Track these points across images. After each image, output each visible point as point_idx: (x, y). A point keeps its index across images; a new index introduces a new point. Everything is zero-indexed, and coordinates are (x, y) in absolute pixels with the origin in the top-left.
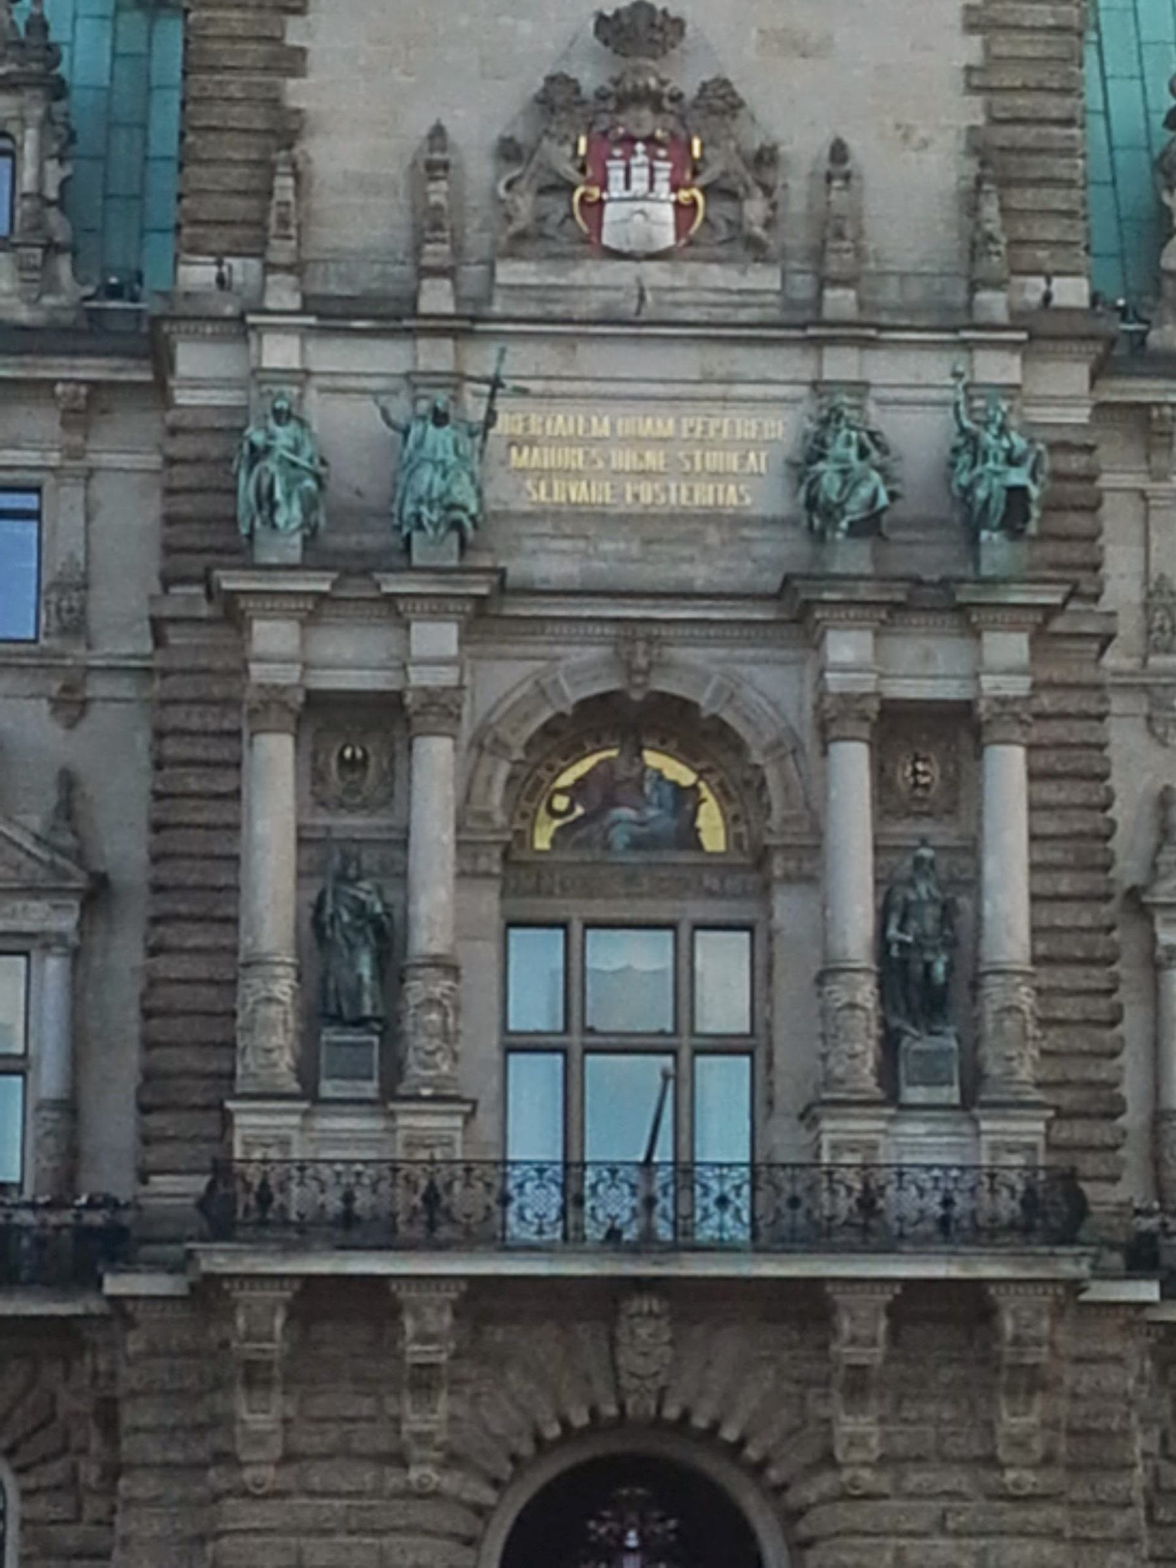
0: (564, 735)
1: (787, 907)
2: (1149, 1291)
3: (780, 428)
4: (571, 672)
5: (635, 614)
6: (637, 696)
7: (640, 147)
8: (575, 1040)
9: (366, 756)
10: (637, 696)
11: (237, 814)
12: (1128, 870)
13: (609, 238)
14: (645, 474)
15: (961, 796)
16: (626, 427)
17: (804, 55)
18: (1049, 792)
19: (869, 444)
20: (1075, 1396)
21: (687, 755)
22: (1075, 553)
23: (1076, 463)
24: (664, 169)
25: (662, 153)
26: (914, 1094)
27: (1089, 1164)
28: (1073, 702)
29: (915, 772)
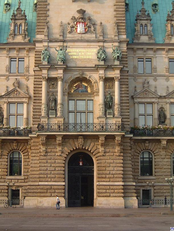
2: (132, 136)
7: (81, 23)
8: (76, 111)
11: (42, 89)
16: (80, 50)
17: (98, 14)
19: (104, 51)
21: (86, 83)
22: (124, 62)
23: (125, 53)
24: (83, 25)
25: (83, 23)
29: (109, 84)
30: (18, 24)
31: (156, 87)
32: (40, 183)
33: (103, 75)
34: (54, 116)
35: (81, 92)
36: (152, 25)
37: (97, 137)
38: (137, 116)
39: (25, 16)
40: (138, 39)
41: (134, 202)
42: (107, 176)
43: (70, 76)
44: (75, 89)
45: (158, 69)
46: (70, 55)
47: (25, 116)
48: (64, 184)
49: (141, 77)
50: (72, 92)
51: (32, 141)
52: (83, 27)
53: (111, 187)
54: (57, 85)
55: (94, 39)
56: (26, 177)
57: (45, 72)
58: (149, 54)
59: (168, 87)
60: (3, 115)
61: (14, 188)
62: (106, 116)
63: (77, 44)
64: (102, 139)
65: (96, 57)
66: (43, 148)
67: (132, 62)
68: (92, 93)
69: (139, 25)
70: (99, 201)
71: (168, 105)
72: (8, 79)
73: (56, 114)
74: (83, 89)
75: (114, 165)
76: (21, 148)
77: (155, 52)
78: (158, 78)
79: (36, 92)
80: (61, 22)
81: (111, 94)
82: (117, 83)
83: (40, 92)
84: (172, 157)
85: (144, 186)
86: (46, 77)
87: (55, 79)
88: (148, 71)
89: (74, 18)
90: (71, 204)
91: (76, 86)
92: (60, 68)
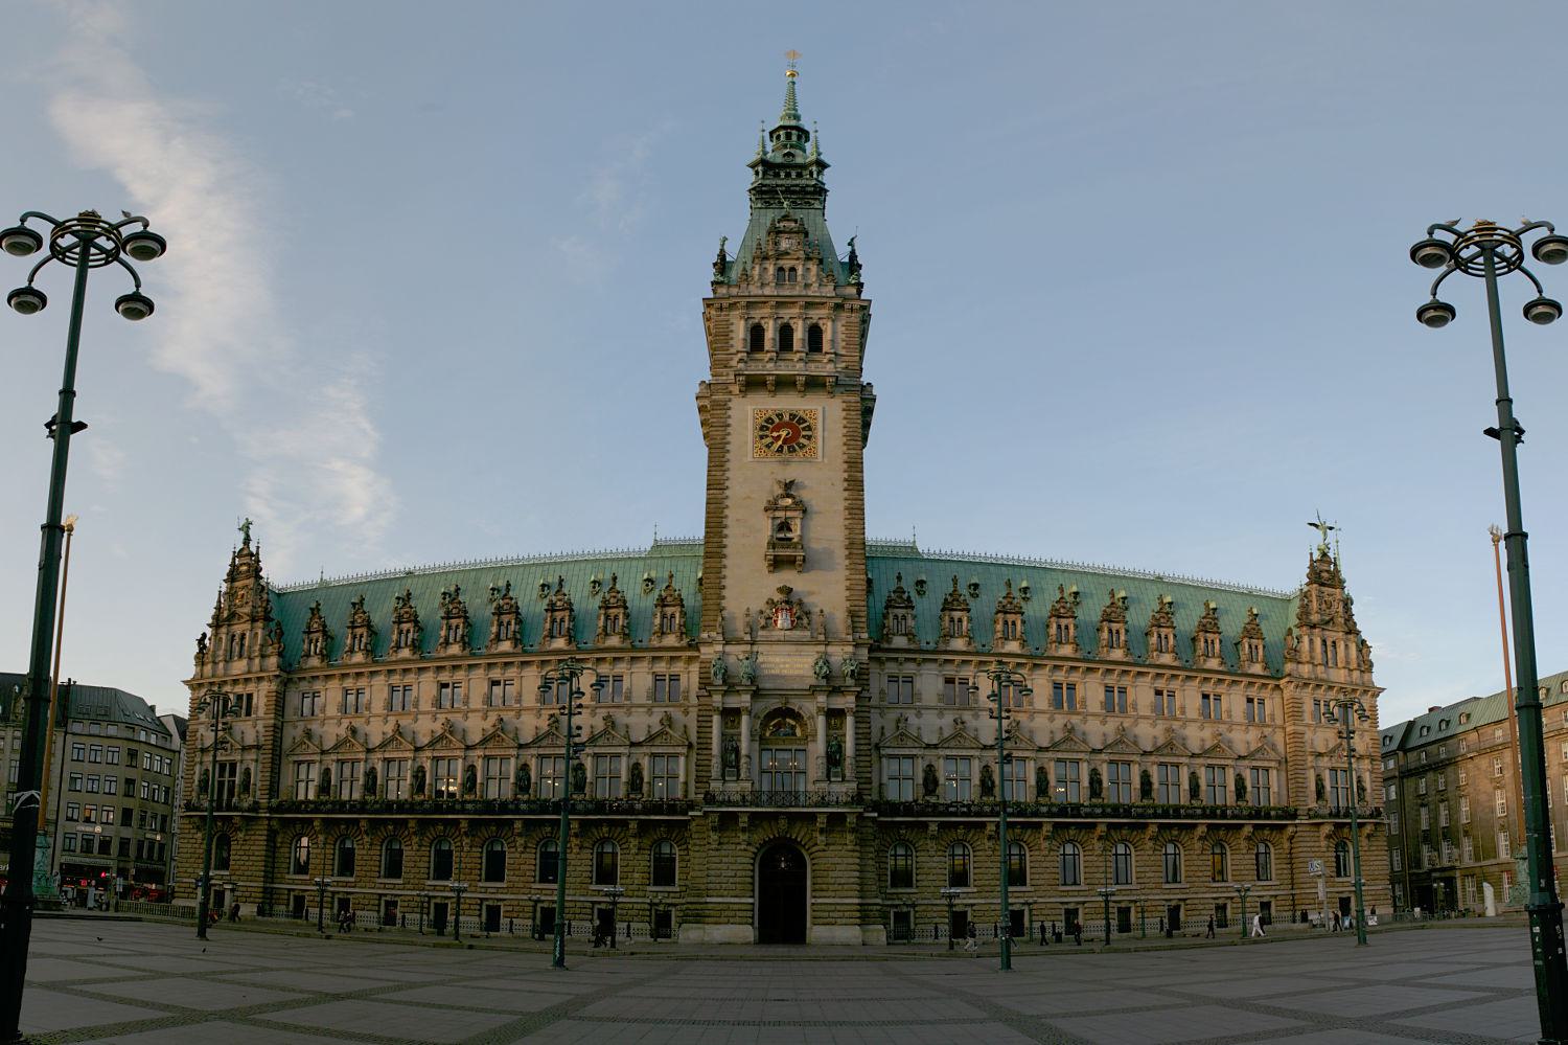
0: (771, 716)
1: (811, 746)
2: (876, 815)
3: (811, 660)
5: (785, 694)
12: (875, 740)
15: (842, 725)
18: (859, 725)
20: (862, 833)
21: (794, 719)
22: (865, 682)
23: (865, 666)
26: (833, 779)
27: (866, 792)
28: (864, 709)
31: (919, 729)
32: (708, 900)
33: (825, 705)
34: (735, 778)
35: (785, 735)
36: (914, 617)
37: (813, 817)
38: (885, 779)
39: (682, 600)
40: (889, 641)
41: (878, 934)
42: (831, 887)
45: (923, 697)
47: (682, 779)
48: (751, 900)
49: (891, 711)
50: (768, 734)
51: (694, 824)
52: (789, 618)
53: (838, 907)
54: (739, 723)
55: (809, 639)
56: (684, 889)
57: (717, 698)
59: (941, 728)
61: (661, 908)
62: (829, 780)
63: (775, 648)
64: (821, 822)
65: (811, 673)
66: (714, 836)
67: (878, 682)
68: (805, 738)
70: (816, 933)
71: (941, 761)
72: (650, 712)
73: (738, 775)
75: (843, 867)
76: (674, 835)
77: (919, 664)
78: (923, 712)
79: (702, 735)
80: (748, 609)
81: (839, 739)
82: (850, 720)
83: (708, 735)
84: (947, 854)
85: (896, 906)
87: (737, 712)
89: (771, 603)
90: (766, 937)
91: (774, 726)
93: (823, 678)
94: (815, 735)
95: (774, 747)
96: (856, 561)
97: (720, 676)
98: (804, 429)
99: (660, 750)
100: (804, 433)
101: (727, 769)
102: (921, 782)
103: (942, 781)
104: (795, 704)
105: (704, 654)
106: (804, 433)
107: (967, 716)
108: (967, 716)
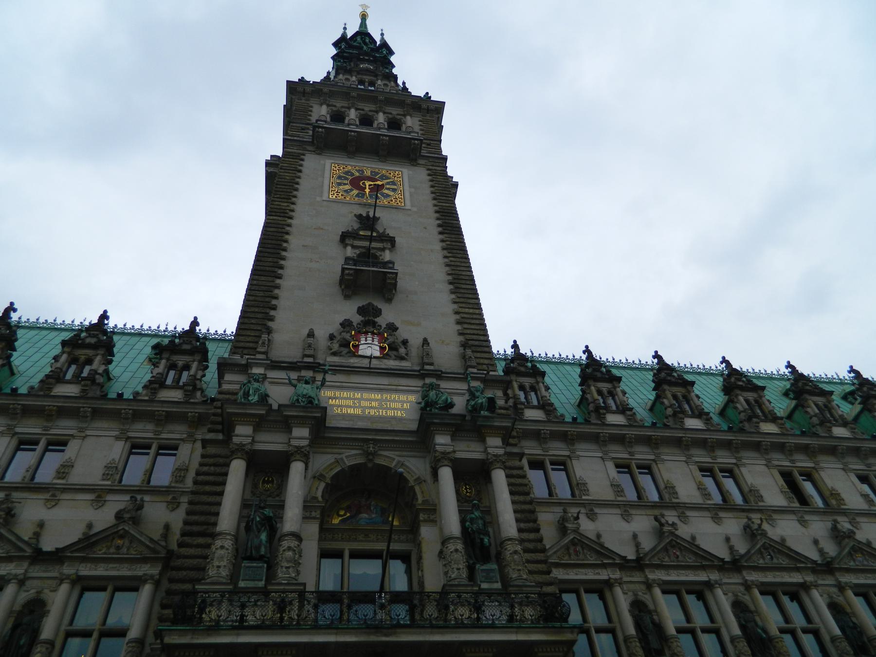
1: (427, 532)
4: (347, 457)
6: (370, 465)
9: (272, 482)
10: (370, 465)
13: (360, 353)
14: (371, 408)
29: (466, 489)
30: (180, 364)
31: (599, 536)
43: (333, 460)
44: (345, 515)
46: (333, 406)
47: (134, 633)
49: (548, 509)
50: (336, 521)
58: (556, 449)
59: (635, 536)
60: (39, 627)
63: (355, 379)
69: (515, 385)
74: (373, 516)
78: (597, 510)
82: (499, 477)
83: (213, 509)
86: (244, 445)
88: (563, 491)
92: (301, 421)
93: (441, 409)
94: (433, 510)
95: (347, 547)
96: (467, 296)
97: (254, 398)
98: (388, 183)
99: (101, 571)
100: (388, 186)
101: (245, 564)
102: (631, 630)
103: (672, 631)
104: (390, 458)
105: (230, 382)
106: (388, 186)
107: (671, 517)
108: (671, 517)
